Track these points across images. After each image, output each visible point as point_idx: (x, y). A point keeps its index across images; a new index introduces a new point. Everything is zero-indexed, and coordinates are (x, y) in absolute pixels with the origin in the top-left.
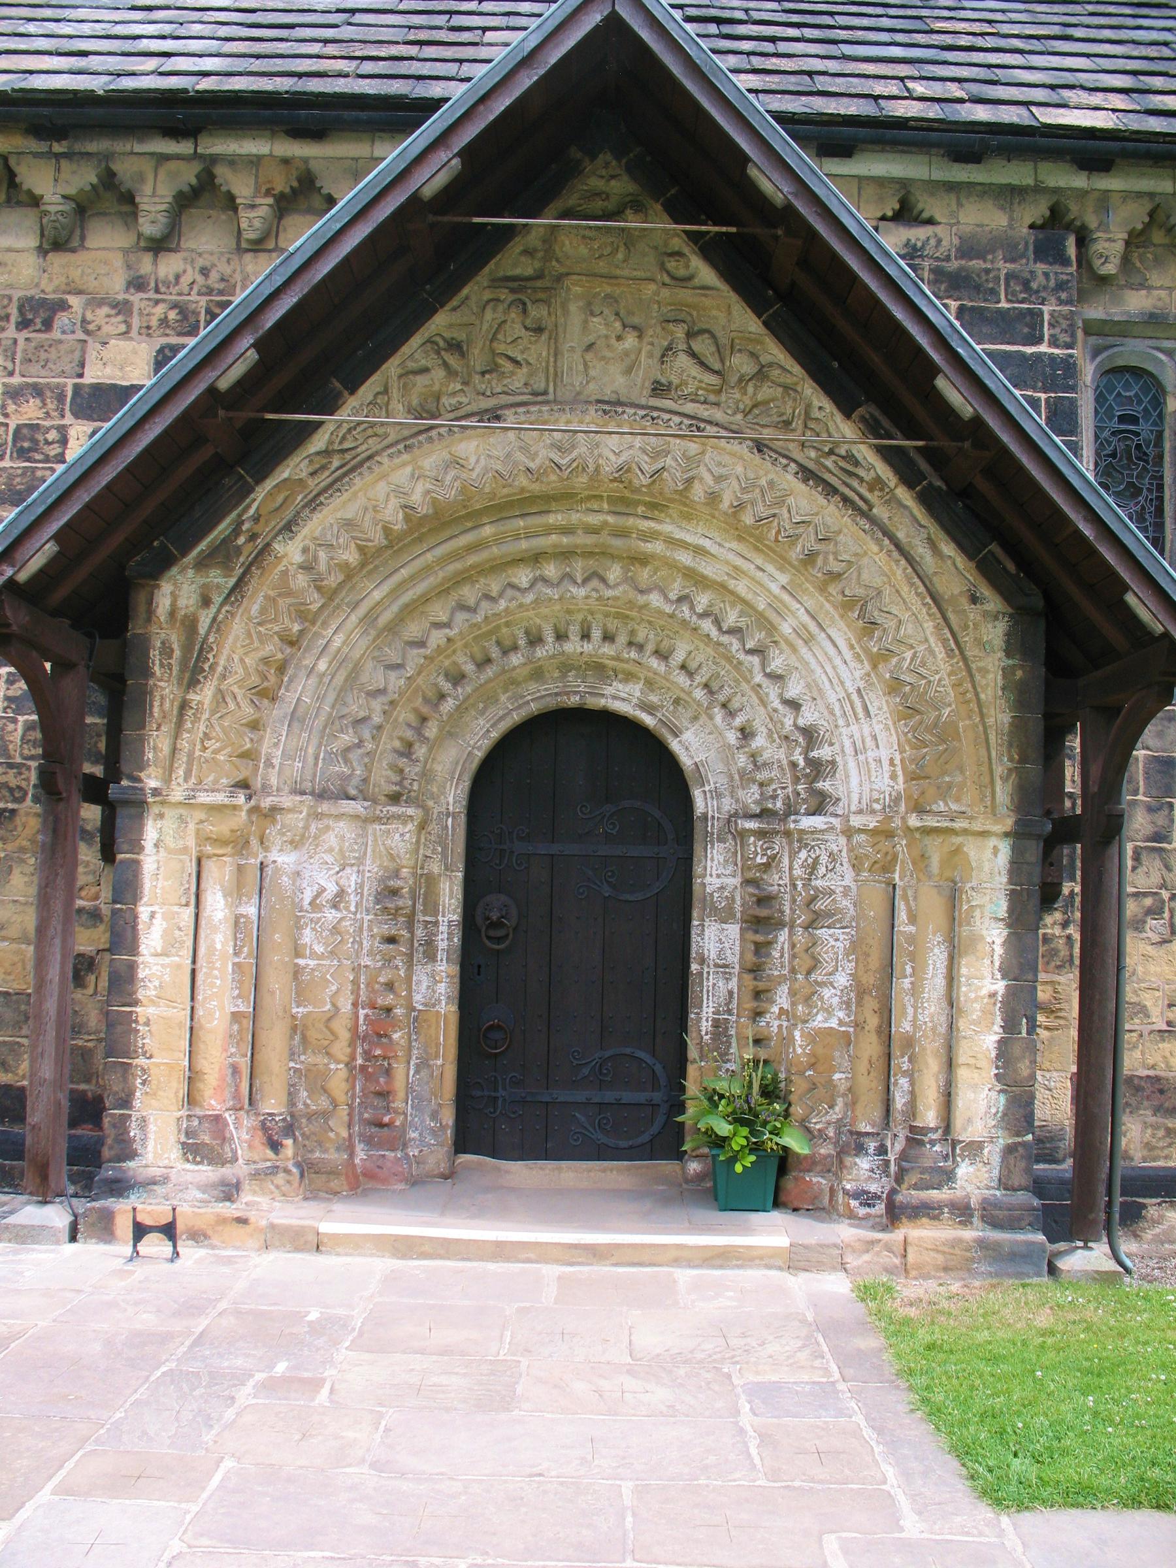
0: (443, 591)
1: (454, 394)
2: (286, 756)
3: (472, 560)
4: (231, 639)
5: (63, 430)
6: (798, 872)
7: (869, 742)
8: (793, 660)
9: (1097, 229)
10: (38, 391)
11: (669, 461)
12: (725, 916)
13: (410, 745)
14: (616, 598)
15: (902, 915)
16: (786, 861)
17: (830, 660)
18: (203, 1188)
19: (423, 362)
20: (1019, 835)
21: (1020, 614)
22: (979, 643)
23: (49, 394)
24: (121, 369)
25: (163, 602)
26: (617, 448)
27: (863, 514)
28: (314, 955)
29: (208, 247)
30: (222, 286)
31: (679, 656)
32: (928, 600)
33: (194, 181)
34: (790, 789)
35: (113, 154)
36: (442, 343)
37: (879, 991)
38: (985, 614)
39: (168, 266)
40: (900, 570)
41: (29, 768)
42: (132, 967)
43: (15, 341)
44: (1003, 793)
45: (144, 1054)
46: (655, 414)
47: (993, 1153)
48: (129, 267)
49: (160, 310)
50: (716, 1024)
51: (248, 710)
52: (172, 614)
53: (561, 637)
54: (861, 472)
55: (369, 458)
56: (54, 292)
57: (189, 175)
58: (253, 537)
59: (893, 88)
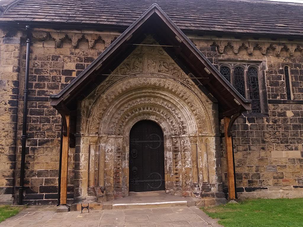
0: (126, 103)
1: (128, 72)
2: (103, 128)
3: (131, 97)
4: (94, 110)
5: (60, 77)
6: (182, 143)
7: (192, 123)
8: (179, 112)
9: (220, 46)
10: (56, 71)
11: (161, 82)
12: (170, 151)
13: (121, 126)
14: (152, 103)
15: (199, 149)
16: (179, 142)
17: (185, 111)
18: (92, 200)
19: (123, 67)
20: (216, 136)
21: (214, 103)
22: (209, 108)
23: (57, 71)
24: (70, 67)
25: (83, 104)
26: (153, 81)
27: (190, 89)
28: (108, 160)
29: (84, 48)
30: (86, 54)
31: (161, 112)
32: (200, 102)
33: (81, 37)
34: (179, 131)
35: (68, 32)
36: (126, 64)
37: (195, 161)
38: (209, 103)
39: (77, 51)
40: (196, 97)
41: (56, 132)
42: (79, 164)
43: (51, 63)
44: (213, 130)
45: (81, 178)
46: (159, 75)
47: (216, 186)
48: (71, 51)
49: (76, 58)
50: (169, 168)
51: (98, 121)
52: (84, 106)
53: (144, 109)
54: (190, 83)
55: (115, 82)
56: (58, 55)
57: (80, 36)
58: (98, 94)
59: (189, 25)
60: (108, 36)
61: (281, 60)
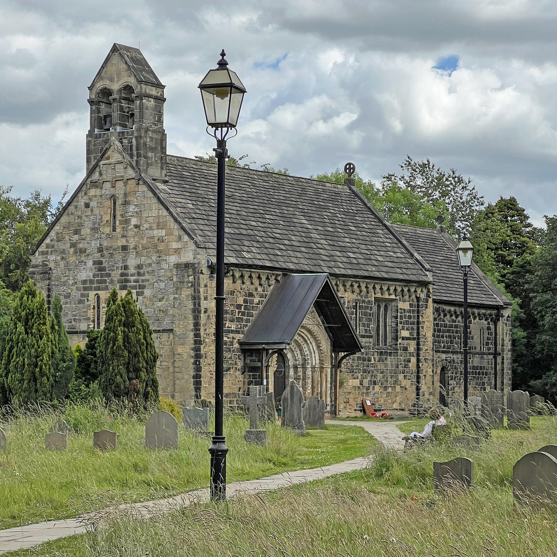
39: (244, 286)
60: (264, 273)
61: (354, 296)
